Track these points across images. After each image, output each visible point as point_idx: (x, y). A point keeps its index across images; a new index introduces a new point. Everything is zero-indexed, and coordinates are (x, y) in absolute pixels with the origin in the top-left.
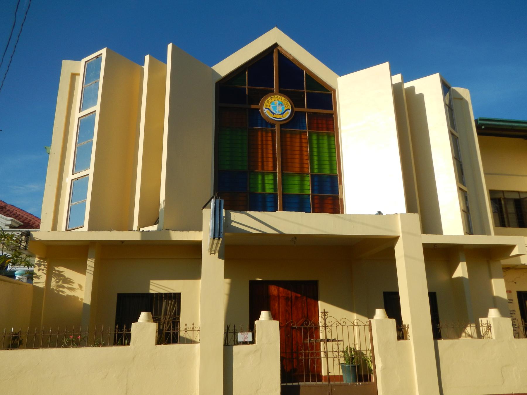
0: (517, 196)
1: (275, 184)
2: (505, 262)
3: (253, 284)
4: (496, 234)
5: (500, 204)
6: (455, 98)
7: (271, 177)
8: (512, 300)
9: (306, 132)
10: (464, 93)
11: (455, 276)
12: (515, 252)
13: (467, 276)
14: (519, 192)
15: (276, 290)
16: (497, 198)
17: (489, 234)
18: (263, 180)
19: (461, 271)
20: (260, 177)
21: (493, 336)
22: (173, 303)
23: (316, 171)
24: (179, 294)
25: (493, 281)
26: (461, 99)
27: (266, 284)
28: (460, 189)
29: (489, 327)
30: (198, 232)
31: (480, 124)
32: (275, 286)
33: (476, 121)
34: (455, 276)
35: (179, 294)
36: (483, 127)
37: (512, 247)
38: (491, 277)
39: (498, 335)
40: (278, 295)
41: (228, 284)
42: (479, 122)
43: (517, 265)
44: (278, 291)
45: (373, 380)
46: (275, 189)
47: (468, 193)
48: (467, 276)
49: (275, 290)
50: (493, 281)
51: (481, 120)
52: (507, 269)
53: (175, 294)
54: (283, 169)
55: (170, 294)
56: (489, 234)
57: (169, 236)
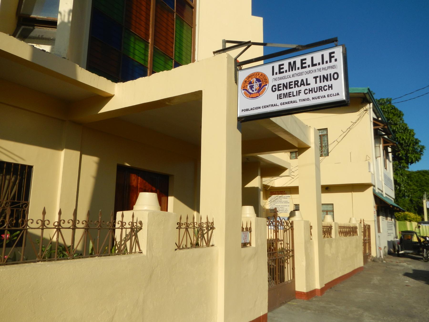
1: (146, 55)
3: (121, 169)
7: (143, 46)
9: (174, 13)
15: (136, 180)
18: (135, 43)
20: (132, 39)
22: (13, 179)
23: (177, 59)
24: (31, 167)
27: (131, 170)
30: (110, 81)
32: (135, 175)
35: (31, 167)
40: (137, 186)
41: (97, 163)
44: (137, 181)
45: (288, 277)
46: (145, 61)
49: (134, 180)
53: (23, 166)
54: (155, 42)
55: (16, 165)
57: (74, 72)
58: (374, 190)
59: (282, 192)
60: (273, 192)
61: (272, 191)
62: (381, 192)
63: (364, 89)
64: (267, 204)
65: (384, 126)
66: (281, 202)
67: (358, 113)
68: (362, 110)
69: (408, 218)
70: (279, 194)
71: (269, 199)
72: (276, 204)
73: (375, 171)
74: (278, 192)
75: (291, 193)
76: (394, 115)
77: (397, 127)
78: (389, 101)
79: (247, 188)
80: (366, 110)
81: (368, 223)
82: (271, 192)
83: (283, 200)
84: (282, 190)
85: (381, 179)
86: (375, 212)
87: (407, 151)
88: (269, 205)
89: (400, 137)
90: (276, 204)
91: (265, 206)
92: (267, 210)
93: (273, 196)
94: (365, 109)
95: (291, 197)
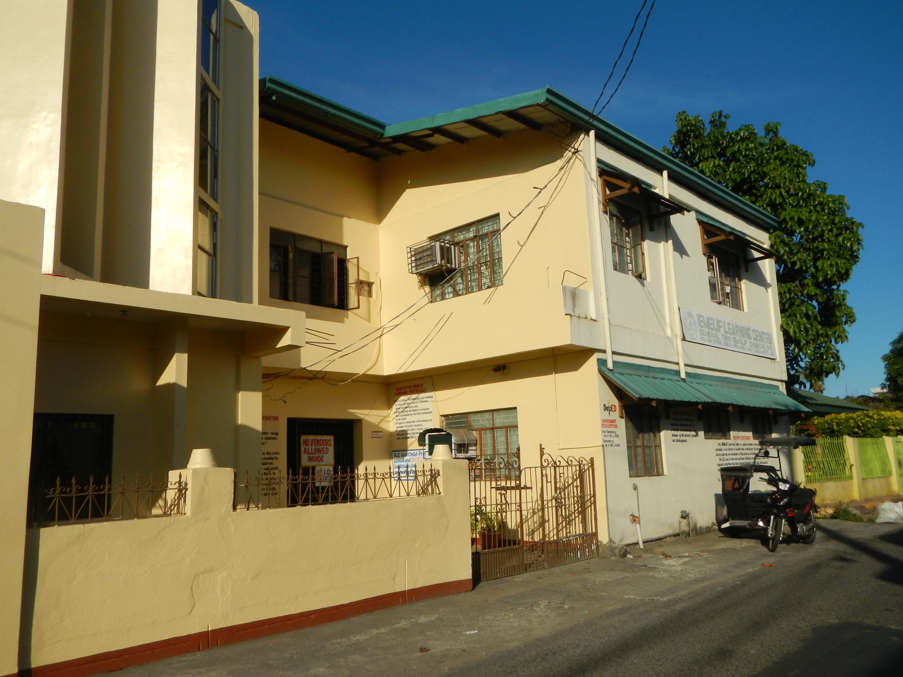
0: (316, 249)
2: (269, 361)
4: (261, 303)
5: (286, 257)
6: (226, 20)
8: (277, 434)
10: (250, 18)
11: (163, 380)
12: (285, 341)
13: (184, 383)
14: (321, 242)
16: (282, 245)
17: (251, 302)
19: (176, 371)
21: (188, 509)
25: (241, 396)
26: (241, 26)
28: (201, 205)
29: (182, 490)
31: (269, 88)
33: (262, 82)
34: (163, 380)
36: (274, 98)
37: (281, 331)
38: (238, 389)
39: (201, 505)
42: (268, 84)
43: (294, 370)
47: (220, 216)
48: (184, 383)
50: (241, 396)
51: (271, 81)
52: (271, 376)
56: (251, 302)
58: (602, 363)
59: (417, 386)
60: (401, 389)
61: (400, 385)
62: (674, 367)
63: (537, 95)
64: (390, 419)
65: (630, 189)
66: (416, 412)
67: (559, 163)
68: (568, 154)
69: (892, 427)
70: (412, 393)
71: (394, 407)
72: (409, 419)
73: (605, 310)
74: (410, 387)
75: (435, 389)
76: (783, 163)
77: (781, 194)
78: (772, 131)
79: (160, 386)
80: (577, 151)
81: (586, 455)
82: (398, 389)
83: (421, 406)
84: (416, 383)
85: (669, 333)
86: (608, 424)
87: (815, 254)
88: (395, 421)
89: (792, 218)
90: (409, 419)
91: (382, 425)
92: (391, 434)
93: (402, 398)
94: (573, 150)
95: (433, 399)
